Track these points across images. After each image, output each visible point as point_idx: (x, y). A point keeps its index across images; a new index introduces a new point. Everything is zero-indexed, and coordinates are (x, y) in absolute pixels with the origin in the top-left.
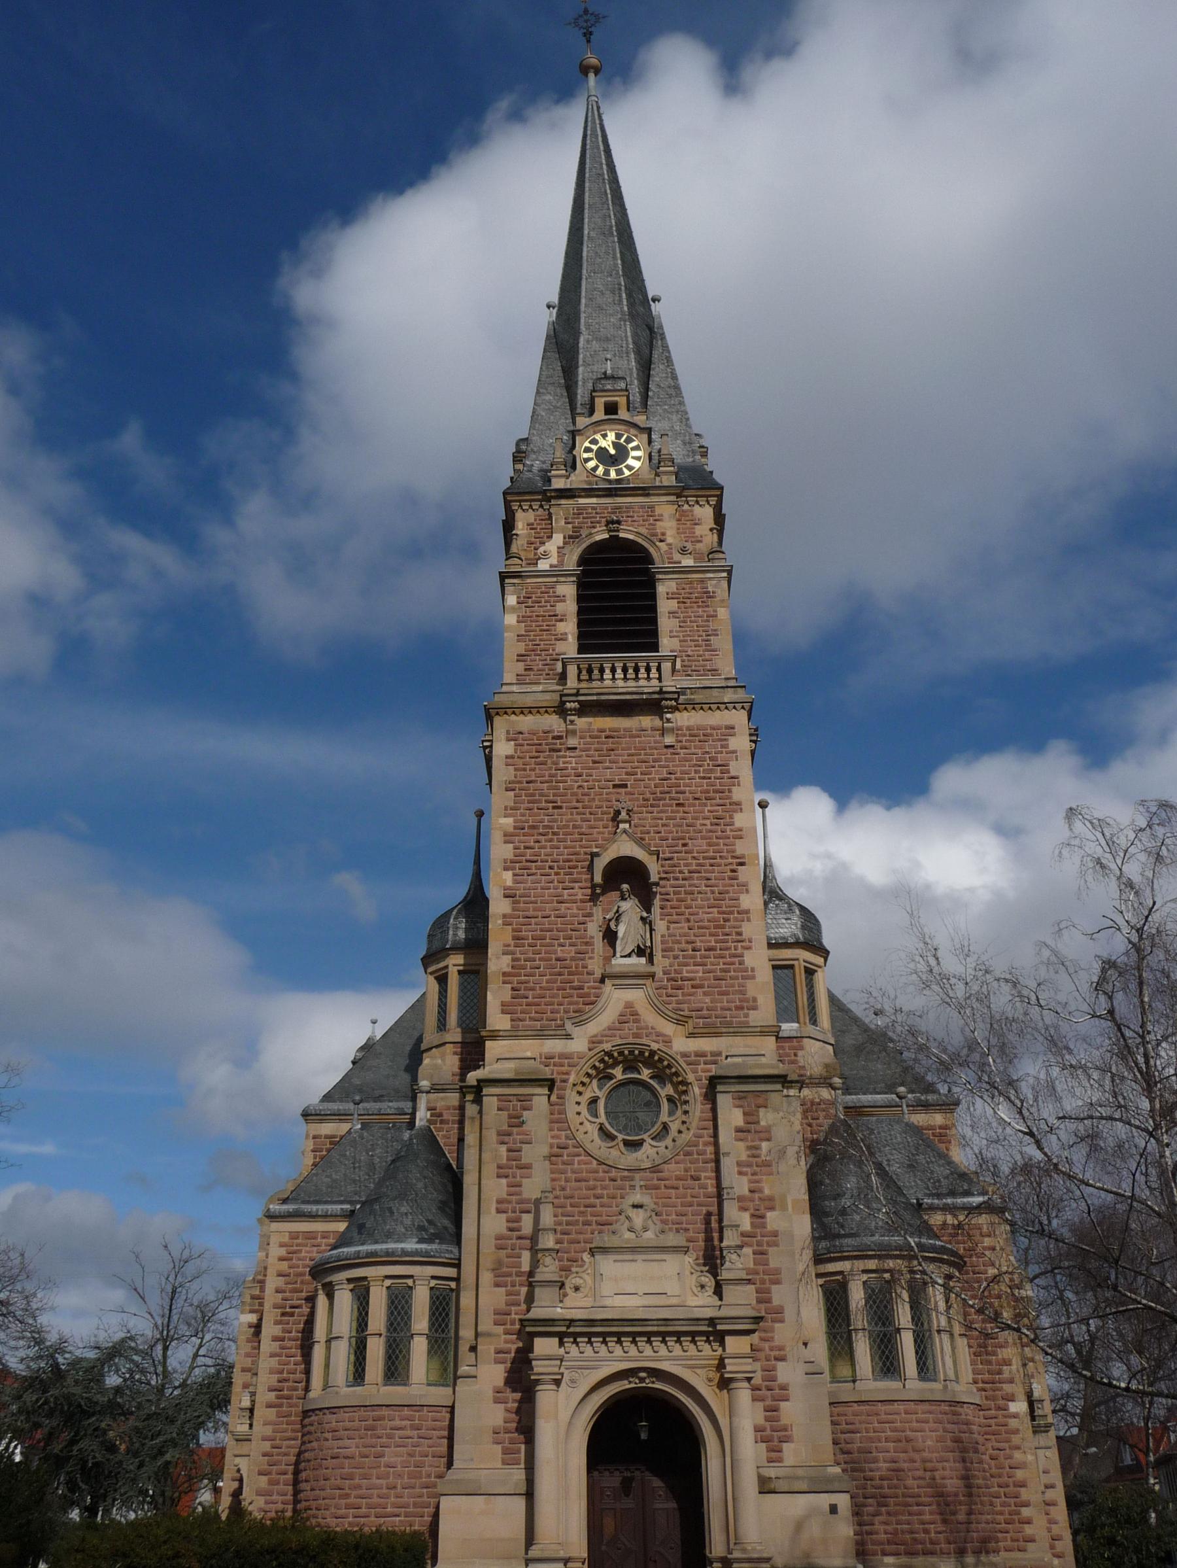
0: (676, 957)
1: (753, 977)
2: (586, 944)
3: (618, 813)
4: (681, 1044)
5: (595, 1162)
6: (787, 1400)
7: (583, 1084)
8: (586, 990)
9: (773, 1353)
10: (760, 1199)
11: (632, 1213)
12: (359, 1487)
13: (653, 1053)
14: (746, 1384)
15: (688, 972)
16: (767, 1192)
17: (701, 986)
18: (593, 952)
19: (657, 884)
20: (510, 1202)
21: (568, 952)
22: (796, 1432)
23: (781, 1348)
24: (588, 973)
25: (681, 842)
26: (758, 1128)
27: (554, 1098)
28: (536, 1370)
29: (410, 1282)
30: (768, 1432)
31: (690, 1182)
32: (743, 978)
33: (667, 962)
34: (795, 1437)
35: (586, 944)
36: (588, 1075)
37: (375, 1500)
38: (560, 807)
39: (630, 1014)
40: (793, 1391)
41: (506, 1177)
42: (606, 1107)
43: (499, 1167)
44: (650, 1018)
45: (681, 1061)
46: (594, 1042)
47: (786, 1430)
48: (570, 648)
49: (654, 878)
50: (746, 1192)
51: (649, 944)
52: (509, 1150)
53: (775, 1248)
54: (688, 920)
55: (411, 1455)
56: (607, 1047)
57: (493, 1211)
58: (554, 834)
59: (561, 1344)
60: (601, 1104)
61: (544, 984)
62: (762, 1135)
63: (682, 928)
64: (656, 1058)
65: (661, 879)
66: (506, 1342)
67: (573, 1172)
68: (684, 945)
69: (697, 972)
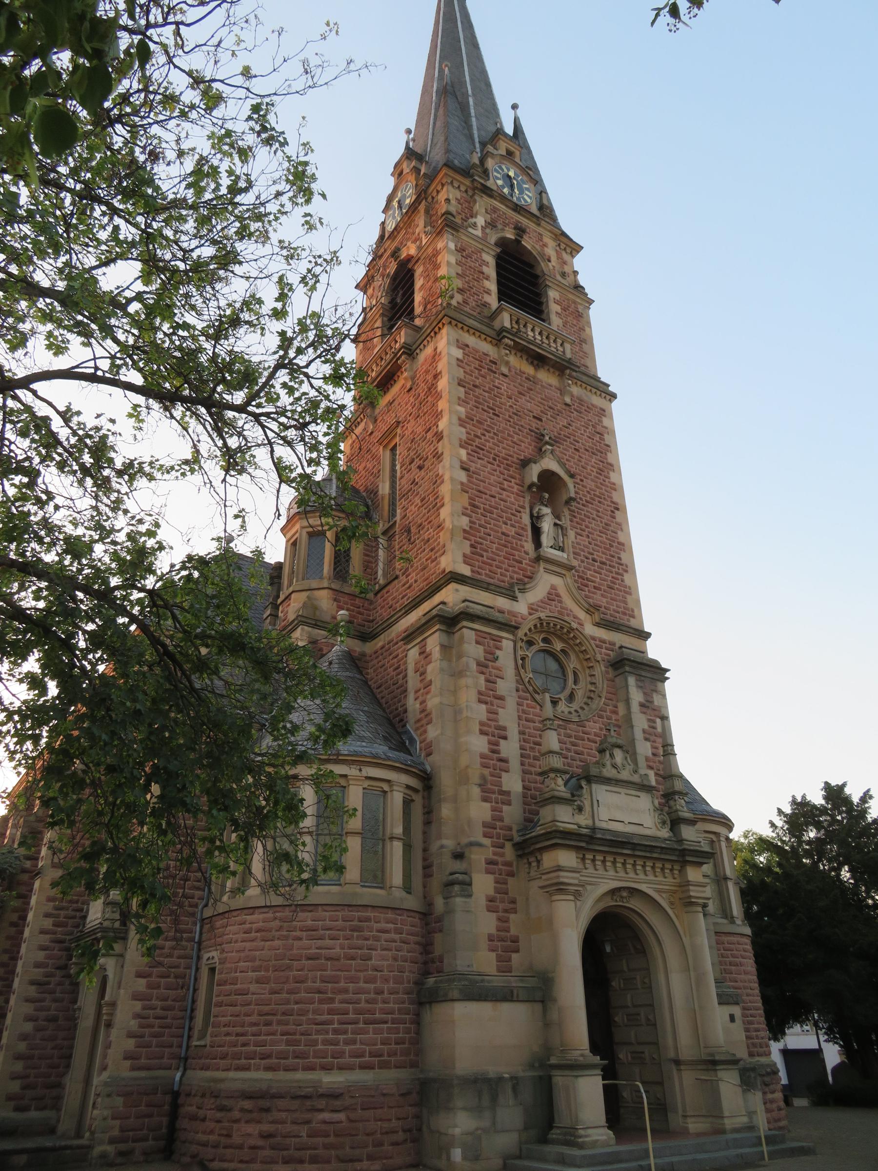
12: (346, 991)
17: (600, 589)
20: (490, 726)
29: (386, 787)
37: (363, 1005)
39: (553, 596)
41: (486, 703)
44: (569, 603)
46: (532, 609)
48: (493, 301)
56: (542, 615)
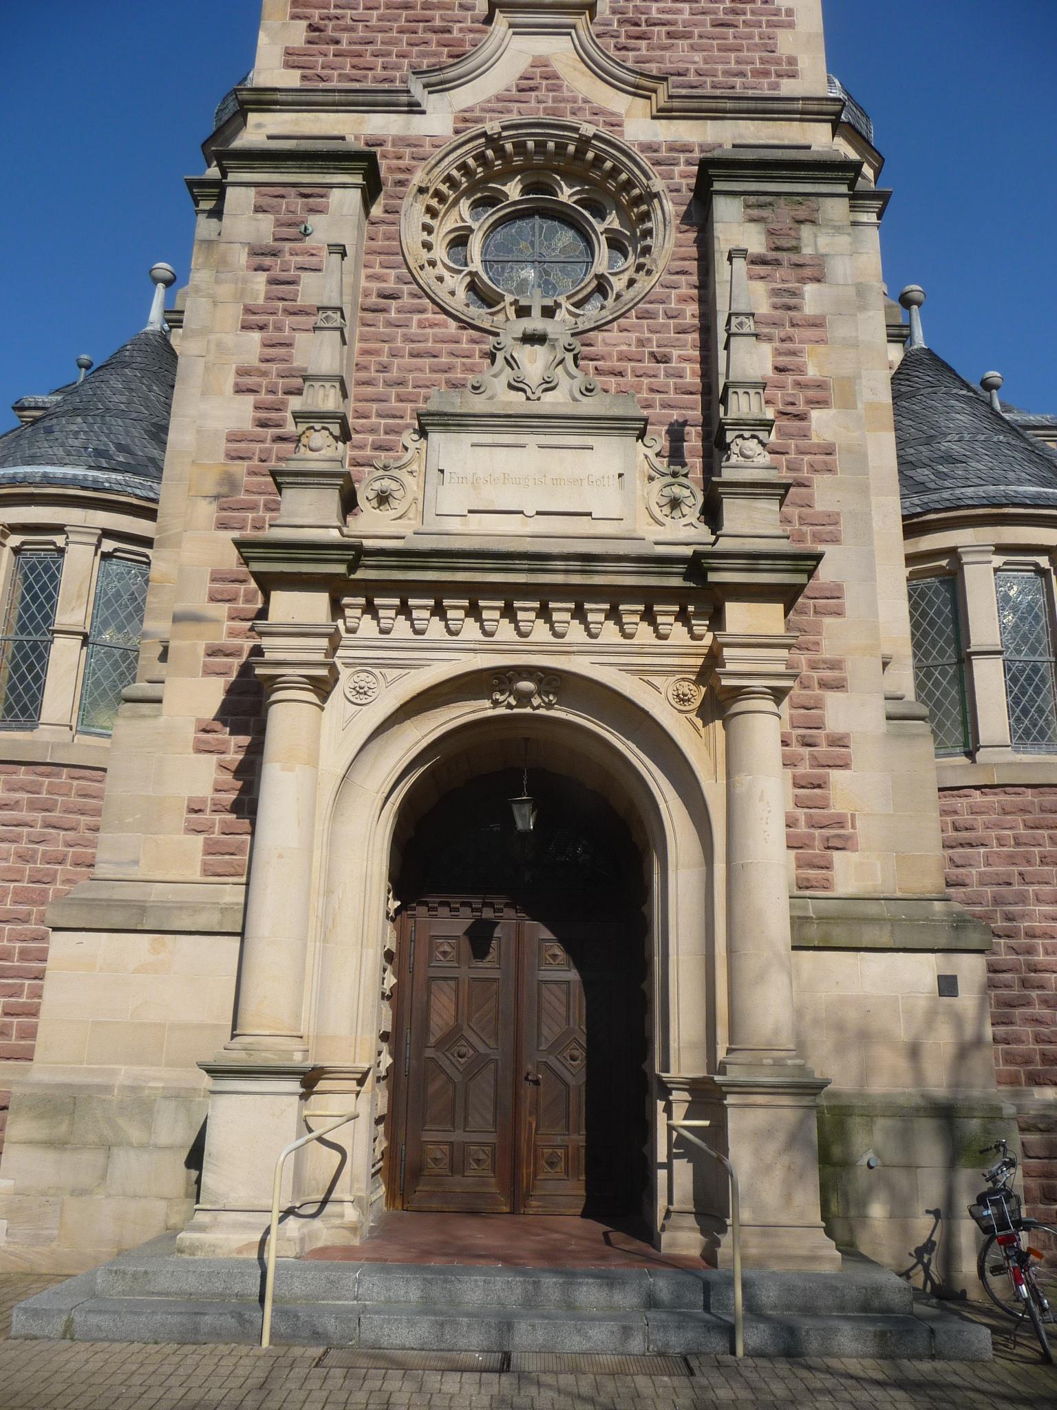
1: (791, 25)
4: (639, 126)
5: (453, 324)
6: (845, 766)
7: (438, 194)
8: (456, 34)
9: (815, 675)
10: (797, 384)
11: (524, 354)
13: (584, 143)
14: (769, 705)
16: (812, 372)
17: (687, 36)
20: (264, 374)
22: (863, 830)
23: (835, 665)
26: (795, 258)
27: (376, 211)
28: (268, 656)
30: (802, 829)
31: (648, 365)
32: (770, 24)
34: (861, 841)
36: (449, 179)
39: (538, 78)
40: (857, 751)
41: (261, 328)
42: (485, 250)
43: (248, 310)
45: (643, 159)
46: (465, 119)
47: (841, 824)
50: (769, 371)
52: (273, 282)
53: (827, 476)
55: (21, 857)
56: (493, 127)
57: (229, 387)
59: (337, 609)
60: (475, 244)
61: (374, 22)
62: (807, 272)
64: (590, 155)
66: (232, 634)
67: (408, 339)
69: (680, 11)
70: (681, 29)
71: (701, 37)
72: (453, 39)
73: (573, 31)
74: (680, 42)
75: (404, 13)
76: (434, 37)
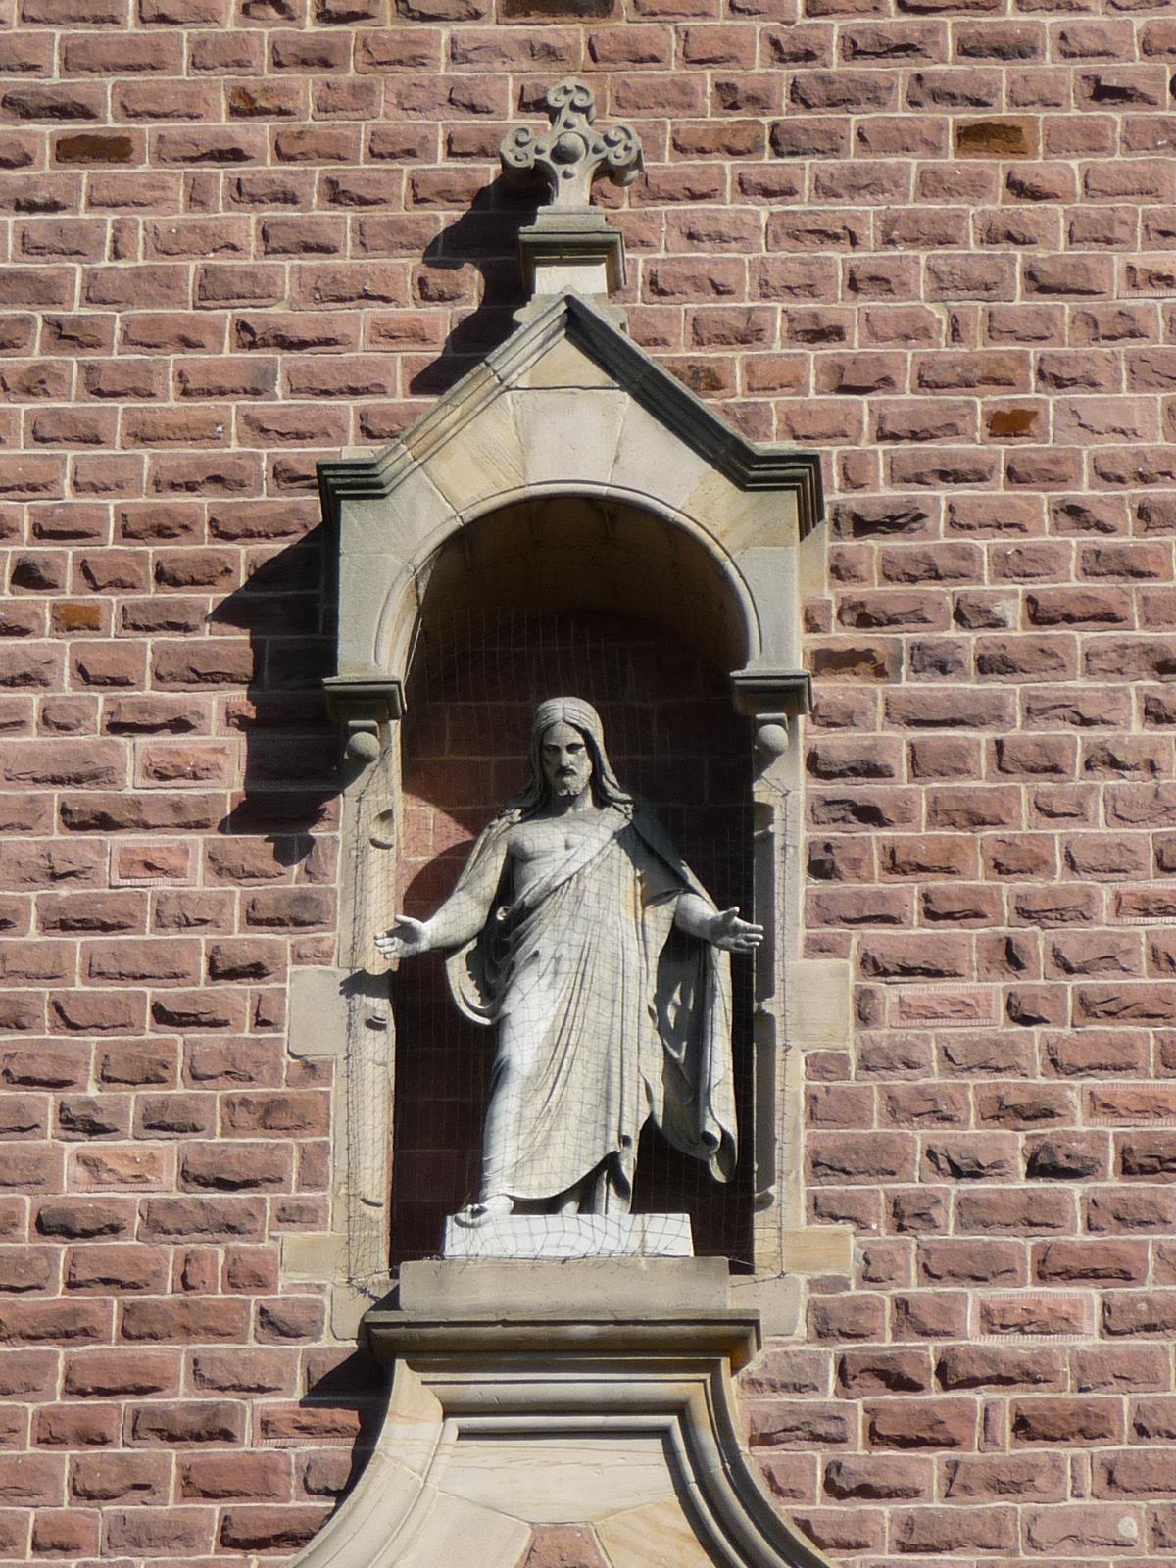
0: (904, 1216)
2: (269, 1114)
3: (528, 187)
15: (990, 1320)
17: (1089, 1427)
18: (312, 1179)
19: (787, 696)
21: (142, 1171)
24: (272, 1325)
25: (986, 401)
33: (845, 1248)
35: (269, 1114)
38: (117, 150)
49: (778, 647)
51: (721, 1117)
54: (1013, 958)
58: (63, 335)
63: (964, 1008)
65: (829, 661)
68: (972, 1135)
69: (1063, 1323)
70: (1070, 1396)
71: (1141, 1431)
72: (238, 1466)
73: (672, 1420)
74: (1065, 1452)
75: (62, 1354)
76: (174, 1455)
